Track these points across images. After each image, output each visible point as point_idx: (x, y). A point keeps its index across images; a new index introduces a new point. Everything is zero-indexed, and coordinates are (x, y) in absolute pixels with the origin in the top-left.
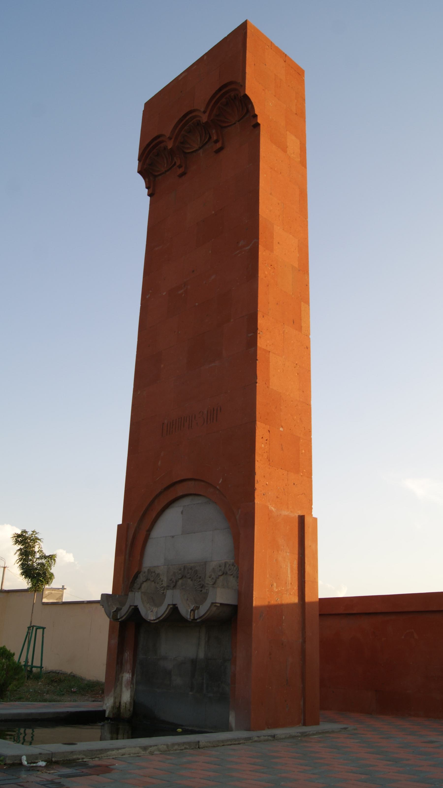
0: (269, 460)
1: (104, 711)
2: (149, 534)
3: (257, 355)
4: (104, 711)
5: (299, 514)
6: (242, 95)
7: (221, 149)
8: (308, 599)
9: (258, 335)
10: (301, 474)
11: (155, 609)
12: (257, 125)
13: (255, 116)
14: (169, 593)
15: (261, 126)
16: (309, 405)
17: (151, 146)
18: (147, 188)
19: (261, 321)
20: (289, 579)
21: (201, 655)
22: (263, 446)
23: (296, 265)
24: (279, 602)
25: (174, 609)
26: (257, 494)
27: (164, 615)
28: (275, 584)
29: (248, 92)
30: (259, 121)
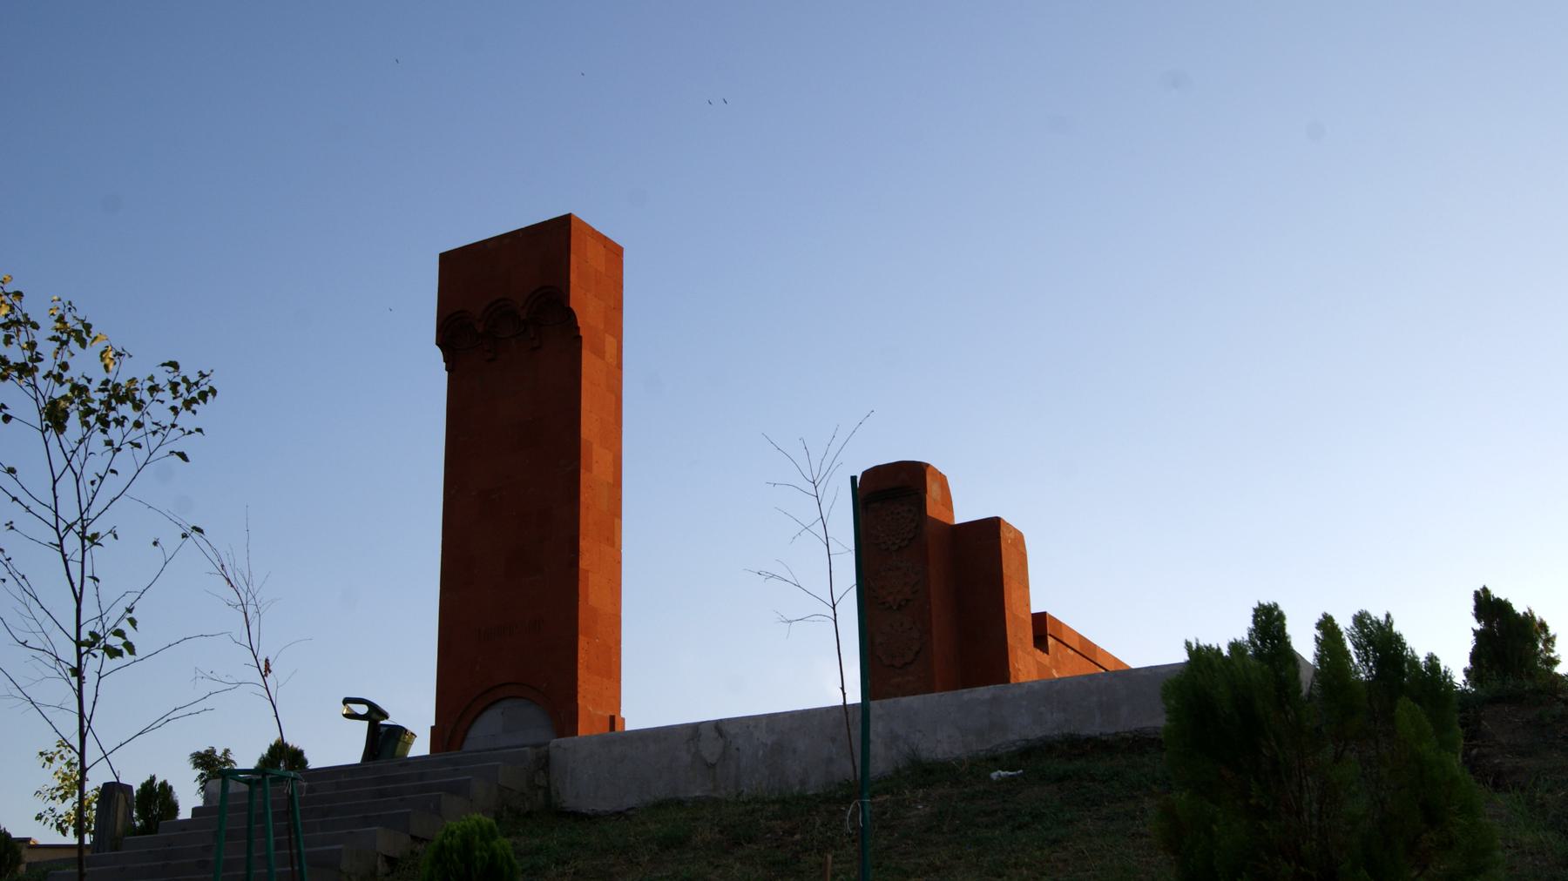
2: (466, 735)
12: (581, 337)
13: (578, 329)
16: (620, 617)
19: (582, 544)
23: (611, 481)
26: (580, 696)
29: (572, 305)
30: (582, 334)
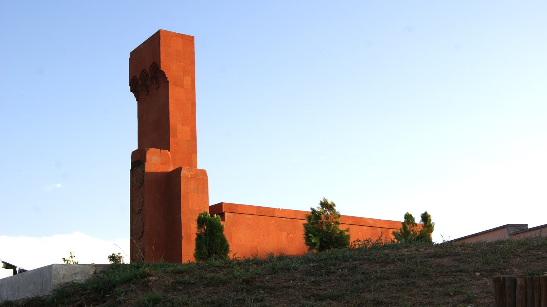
12: (168, 81)
15: (170, 82)
18: (135, 97)
23: (189, 138)
29: (162, 69)
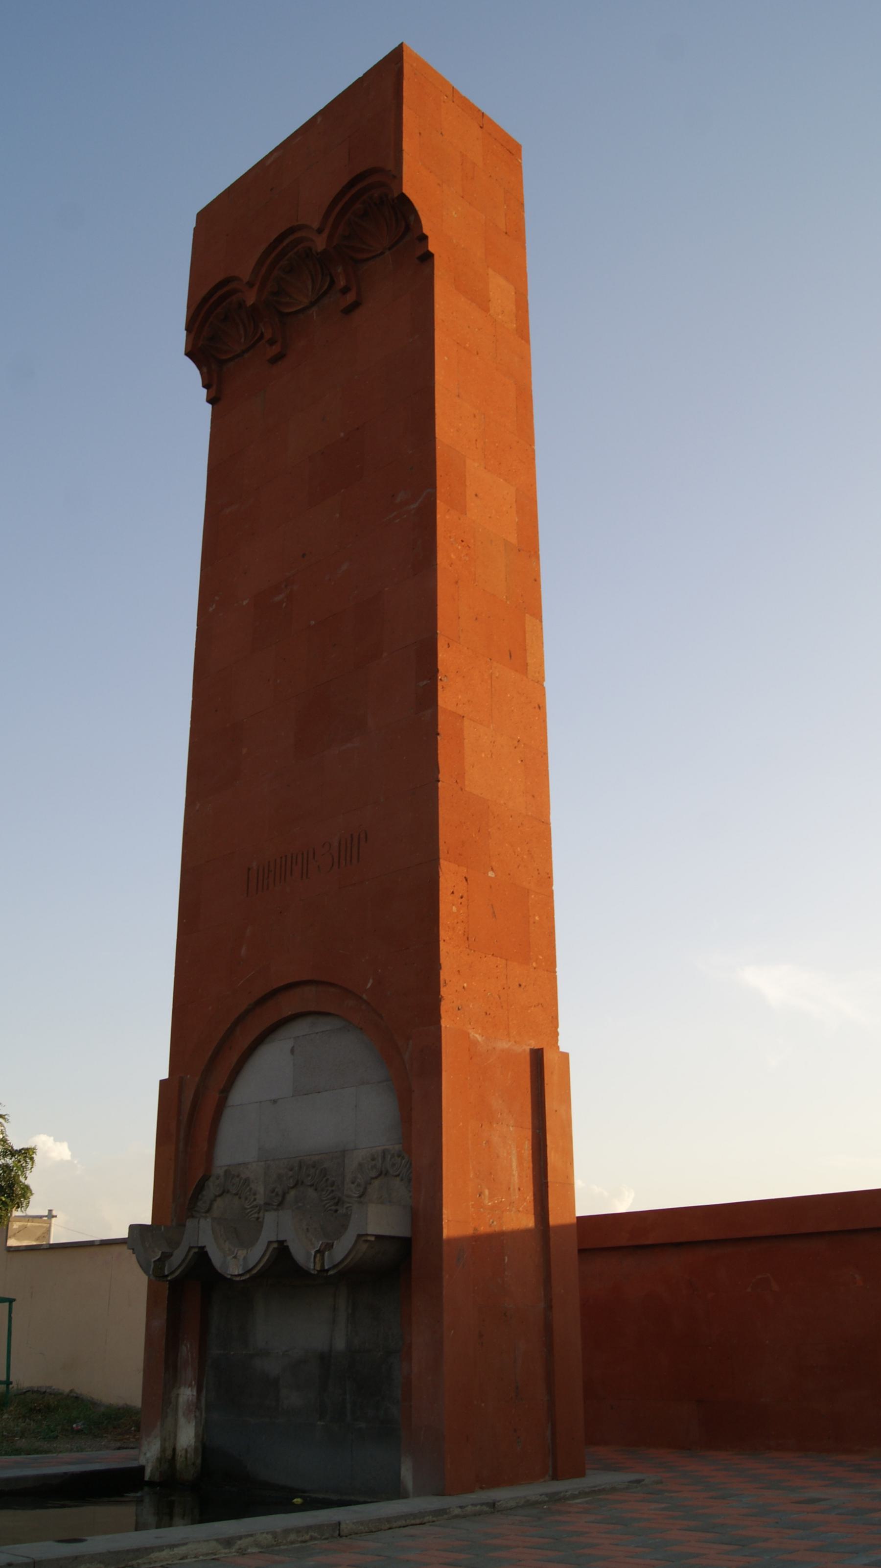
0: (468, 938)
1: (142, 1469)
3: (437, 725)
4: (142, 1469)
5: (532, 1047)
6: (396, 195)
7: (356, 305)
8: (555, 1219)
9: (440, 684)
10: (534, 965)
11: (242, 1253)
12: (428, 257)
13: (424, 238)
14: (269, 1218)
15: (436, 257)
16: (547, 824)
17: (212, 301)
18: (204, 386)
19: (443, 655)
20: (516, 1179)
21: (340, 1344)
22: (454, 909)
23: (513, 539)
24: (496, 1227)
25: (282, 1251)
26: (445, 1008)
27: (261, 1265)
28: (487, 1192)
29: (408, 190)
30: (432, 248)
